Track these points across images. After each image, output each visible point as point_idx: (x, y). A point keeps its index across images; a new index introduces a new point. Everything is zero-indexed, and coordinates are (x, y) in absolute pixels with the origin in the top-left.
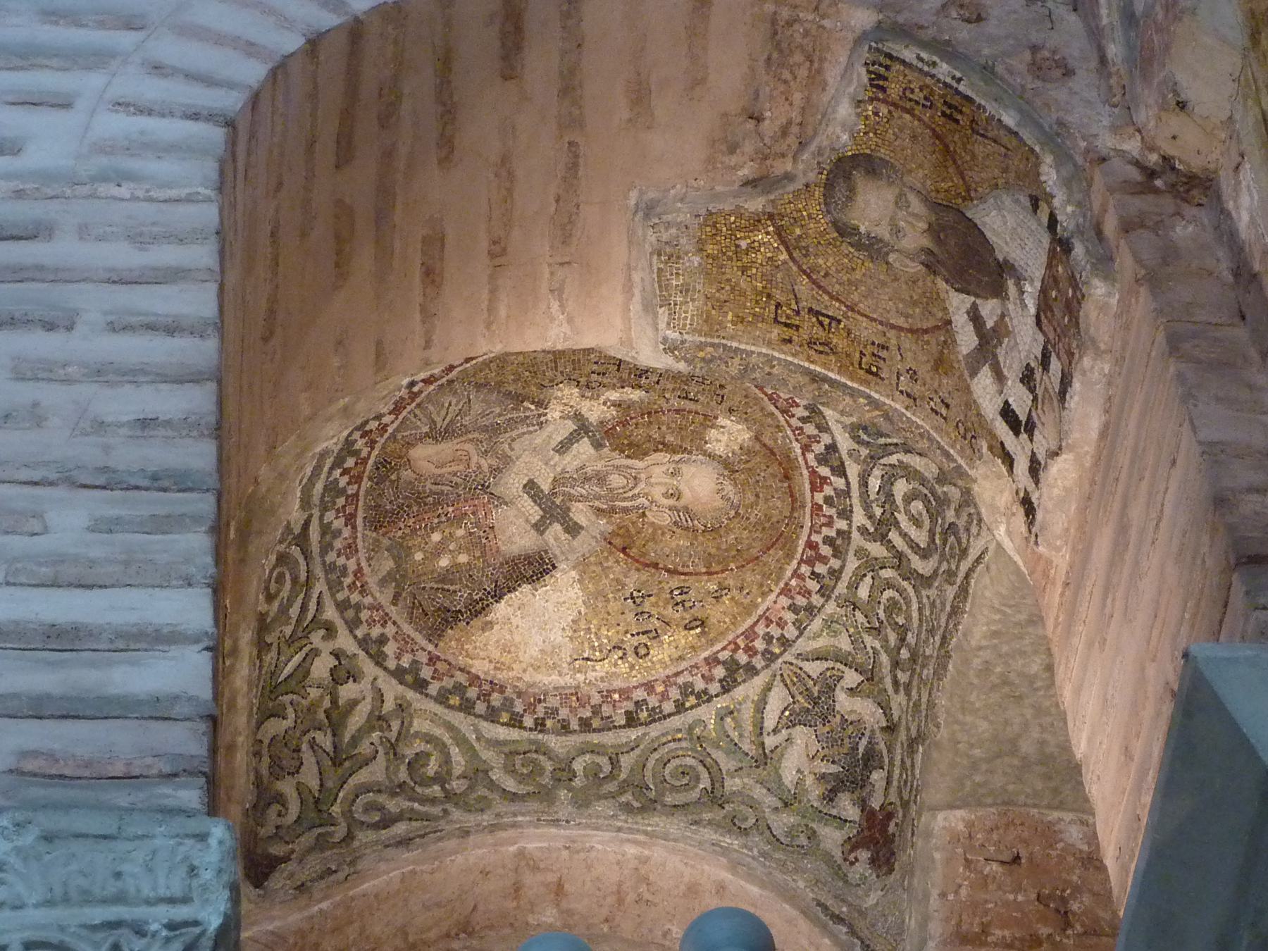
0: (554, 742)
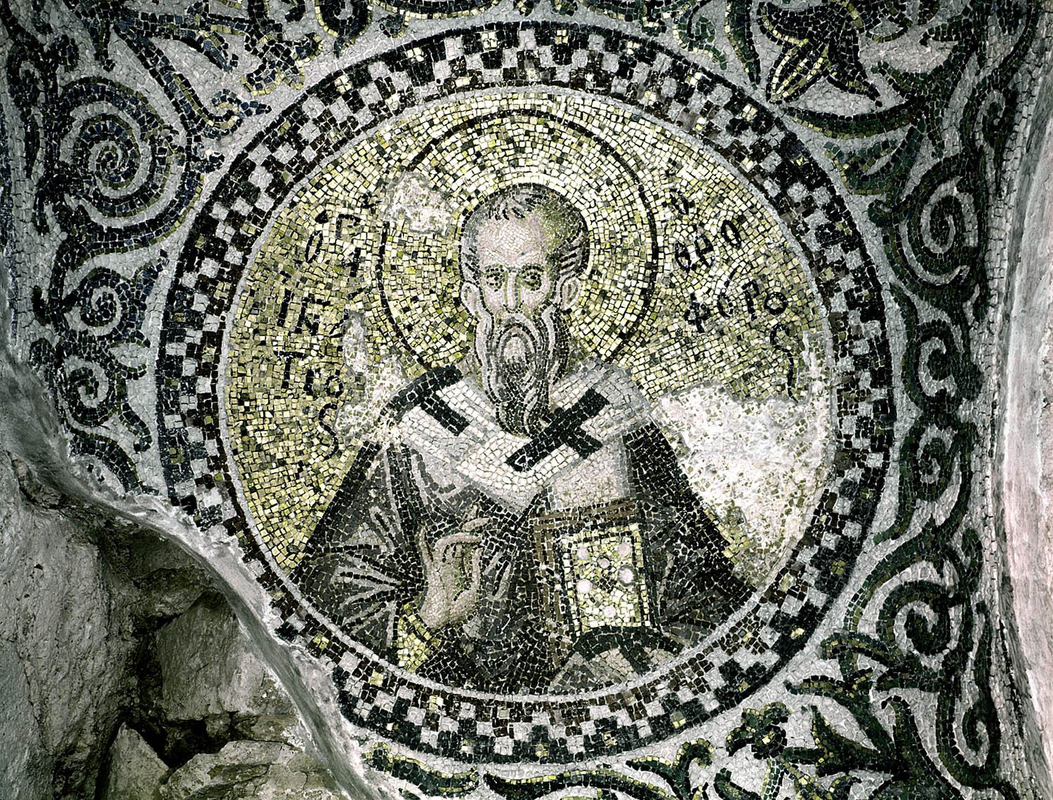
0: (902, 427)
